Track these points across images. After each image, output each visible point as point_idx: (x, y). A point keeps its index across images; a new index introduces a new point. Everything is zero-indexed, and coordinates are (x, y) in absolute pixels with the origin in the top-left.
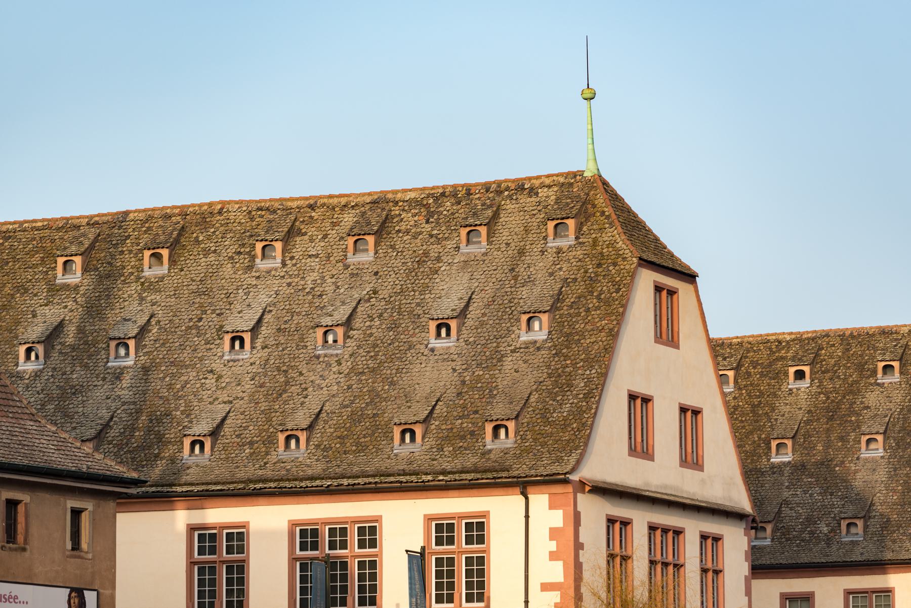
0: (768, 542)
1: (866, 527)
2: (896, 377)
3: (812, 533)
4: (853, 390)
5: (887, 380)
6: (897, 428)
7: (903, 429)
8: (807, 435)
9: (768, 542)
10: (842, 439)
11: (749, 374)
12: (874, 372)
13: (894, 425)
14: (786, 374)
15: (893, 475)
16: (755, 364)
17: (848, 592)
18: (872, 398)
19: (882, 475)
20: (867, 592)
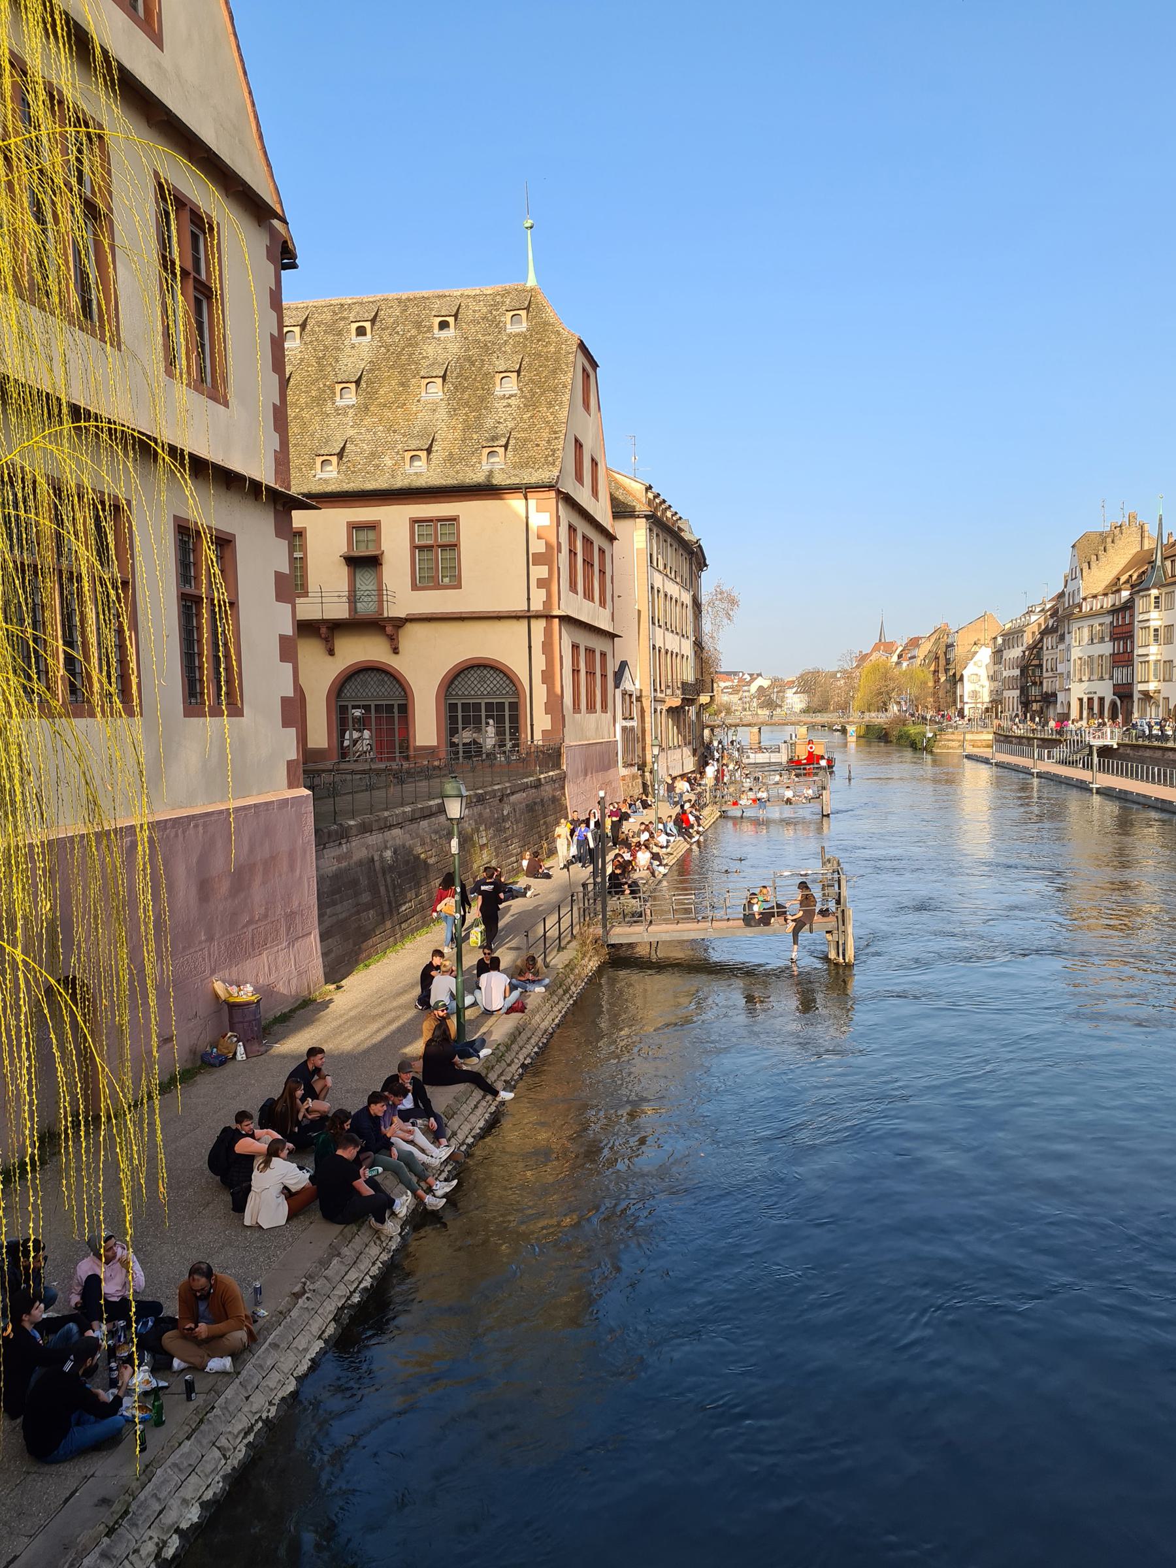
0: (334, 475)
1: (429, 460)
2: (451, 332)
3: (377, 466)
4: (412, 343)
5: (444, 334)
6: (455, 375)
7: (459, 375)
8: (370, 383)
9: (334, 475)
10: (403, 384)
11: (313, 332)
12: (431, 327)
13: (452, 372)
14: (348, 331)
15: (453, 413)
16: (319, 324)
17: (414, 521)
18: (430, 350)
19: (442, 413)
20: (431, 521)
